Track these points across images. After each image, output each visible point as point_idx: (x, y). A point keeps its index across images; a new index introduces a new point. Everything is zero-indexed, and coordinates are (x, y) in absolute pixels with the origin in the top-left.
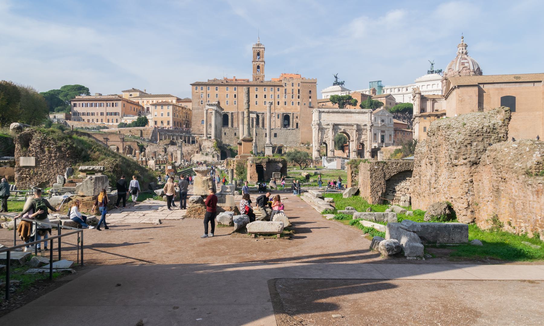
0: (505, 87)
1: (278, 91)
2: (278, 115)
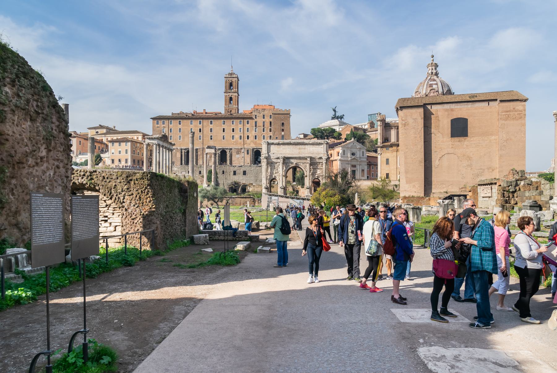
0: (456, 107)
1: (248, 123)
2: (248, 151)
